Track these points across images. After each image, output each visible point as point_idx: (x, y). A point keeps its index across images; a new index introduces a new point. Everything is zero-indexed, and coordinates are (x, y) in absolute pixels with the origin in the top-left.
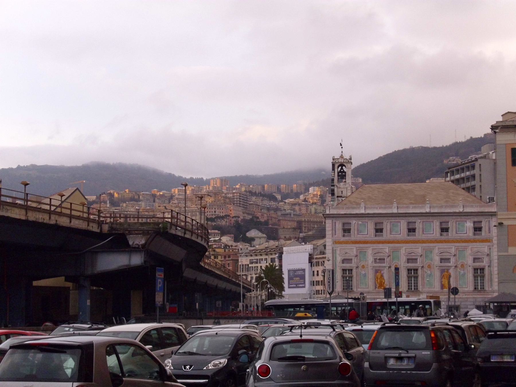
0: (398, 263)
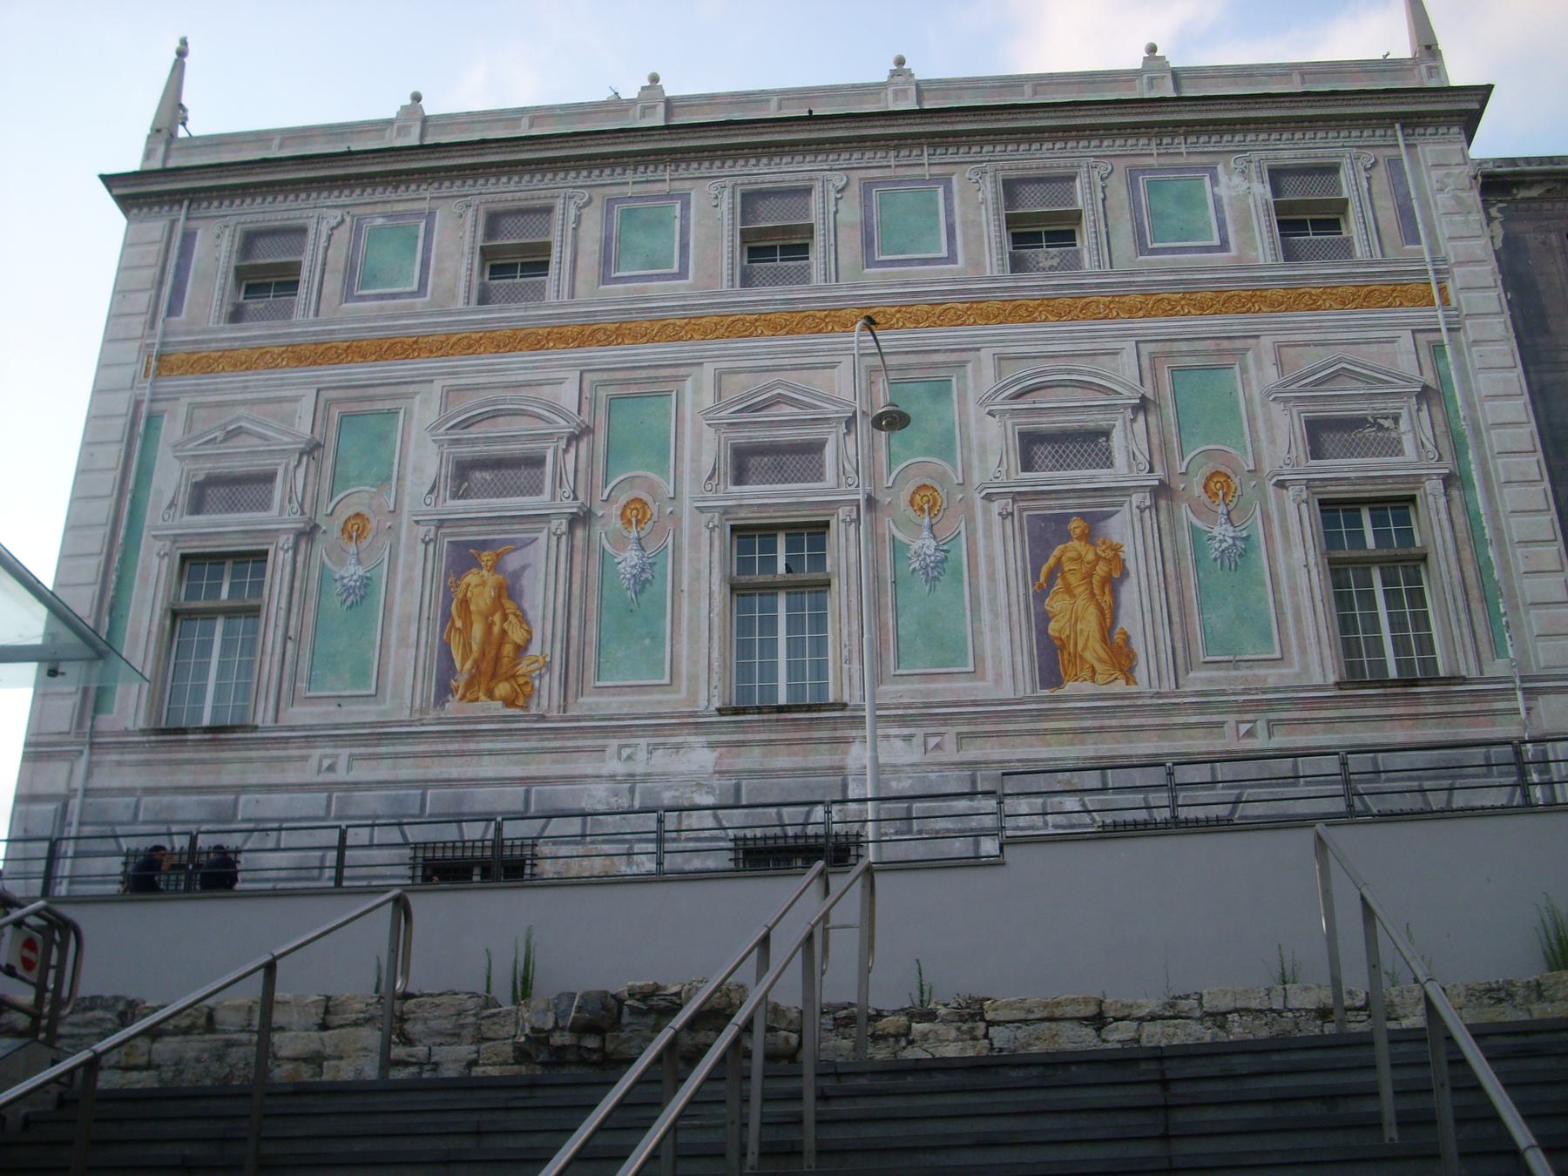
0: (652, 489)
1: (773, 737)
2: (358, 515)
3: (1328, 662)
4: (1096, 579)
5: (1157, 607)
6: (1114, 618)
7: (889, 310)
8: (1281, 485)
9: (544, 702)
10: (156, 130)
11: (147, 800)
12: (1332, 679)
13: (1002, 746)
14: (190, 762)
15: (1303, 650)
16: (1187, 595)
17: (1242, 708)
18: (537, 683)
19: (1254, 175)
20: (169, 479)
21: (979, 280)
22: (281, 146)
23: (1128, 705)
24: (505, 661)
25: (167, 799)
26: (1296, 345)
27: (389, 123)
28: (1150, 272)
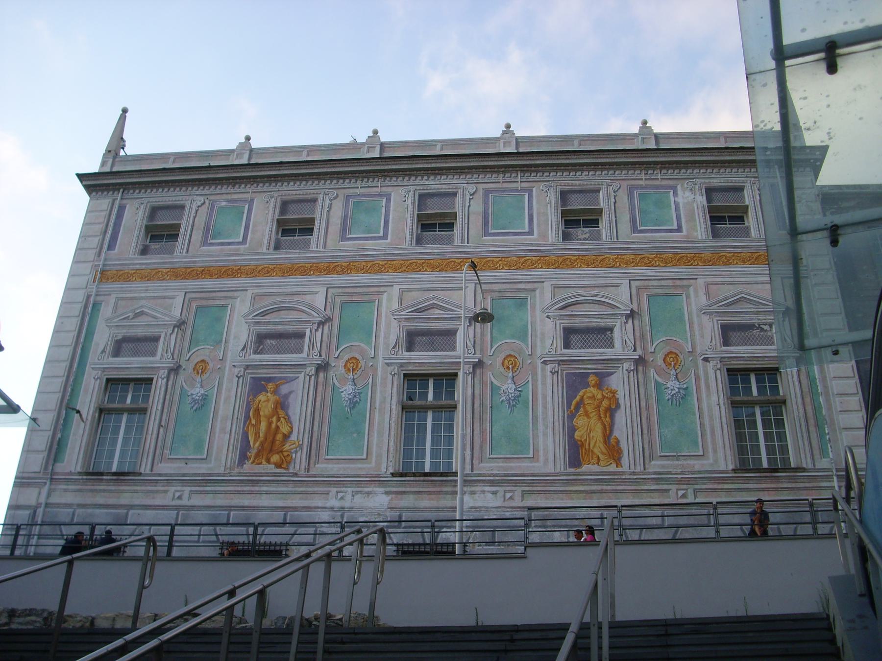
1: (421, 489)
2: (203, 361)
3: (729, 458)
4: (602, 409)
5: (635, 425)
6: (611, 431)
7: (495, 260)
8: (706, 360)
9: (297, 466)
10: (108, 151)
11: (79, 511)
12: (731, 467)
13: (547, 499)
14: (104, 491)
15: (715, 451)
16: (652, 419)
17: (681, 481)
18: (294, 455)
19: (697, 191)
20: (103, 337)
21: (546, 245)
22: (174, 162)
23: (616, 478)
24: (277, 443)
25: (90, 511)
26: (717, 284)
27: (232, 151)
28: (639, 242)
